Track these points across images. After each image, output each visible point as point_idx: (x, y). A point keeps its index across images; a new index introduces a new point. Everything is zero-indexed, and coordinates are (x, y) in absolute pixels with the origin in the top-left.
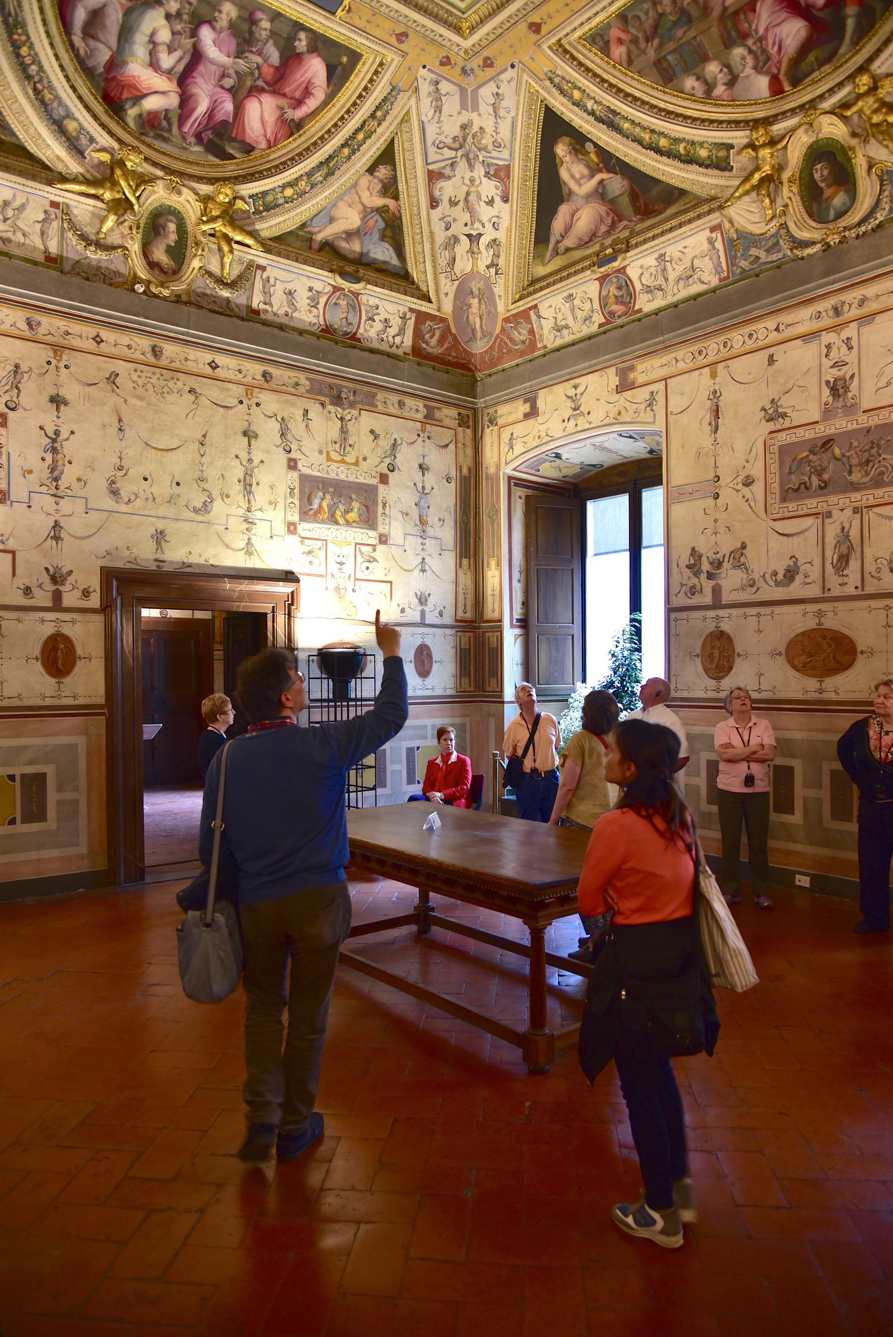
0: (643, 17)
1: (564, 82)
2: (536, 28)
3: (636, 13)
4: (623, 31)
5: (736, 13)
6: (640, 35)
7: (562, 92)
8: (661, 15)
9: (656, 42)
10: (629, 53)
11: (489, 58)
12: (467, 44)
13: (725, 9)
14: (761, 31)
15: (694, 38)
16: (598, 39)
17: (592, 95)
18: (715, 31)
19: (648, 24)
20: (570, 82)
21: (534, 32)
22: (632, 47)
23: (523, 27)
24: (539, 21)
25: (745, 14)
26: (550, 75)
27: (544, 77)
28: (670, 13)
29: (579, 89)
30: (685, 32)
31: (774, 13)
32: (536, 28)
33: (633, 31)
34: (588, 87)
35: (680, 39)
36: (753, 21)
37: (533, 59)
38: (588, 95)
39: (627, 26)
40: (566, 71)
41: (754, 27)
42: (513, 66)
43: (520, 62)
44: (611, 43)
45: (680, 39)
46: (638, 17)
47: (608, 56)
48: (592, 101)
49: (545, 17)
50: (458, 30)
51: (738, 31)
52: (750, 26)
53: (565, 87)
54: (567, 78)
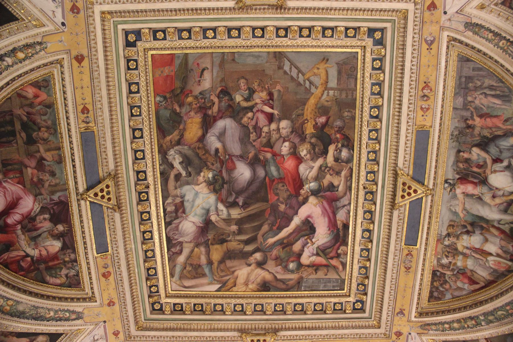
0: (44, 118)
1: (34, 52)
2: (80, 59)
3: (48, 115)
4: (42, 102)
5: (21, 172)
6: (34, 111)
7: (28, 46)
8: (39, 129)
9: (25, 119)
10: (25, 98)
11: (78, 13)
12: (97, 9)
13: (26, 167)
14: (4, 184)
15: (17, 143)
16: (45, 84)
17: (16, 67)
18: (15, 156)
19: (38, 119)
20: (32, 56)
21: (77, 56)
22: (28, 102)
23: (85, 53)
24: (82, 64)
25: (19, 177)
26: (44, 46)
27: (44, 40)
28: (38, 134)
29: (24, 60)
30: (22, 138)
31: (13, 194)
32: (80, 59)
33: (39, 108)
34: (23, 67)
35: (20, 133)
36: (12, 181)
37: (61, 41)
38: (17, 63)
39: (43, 106)
40: (42, 58)
41: (9, 180)
42: (63, 24)
43: (64, 31)
44: (38, 90)
45: (20, 133)
46: (46, 115)
47: (31, 84)
48: (10, 64)
49: (82, 69)
50: (110, 13)
51: (10, 170)
52: (10, 179)
53: (30, 50)
54: (36, 56)
